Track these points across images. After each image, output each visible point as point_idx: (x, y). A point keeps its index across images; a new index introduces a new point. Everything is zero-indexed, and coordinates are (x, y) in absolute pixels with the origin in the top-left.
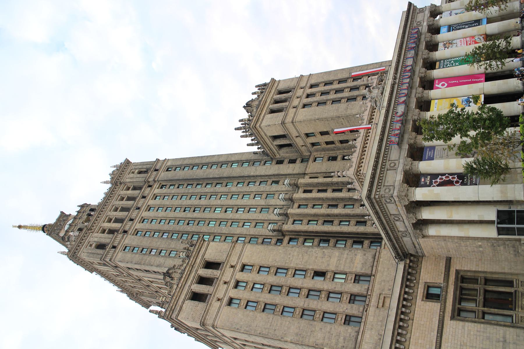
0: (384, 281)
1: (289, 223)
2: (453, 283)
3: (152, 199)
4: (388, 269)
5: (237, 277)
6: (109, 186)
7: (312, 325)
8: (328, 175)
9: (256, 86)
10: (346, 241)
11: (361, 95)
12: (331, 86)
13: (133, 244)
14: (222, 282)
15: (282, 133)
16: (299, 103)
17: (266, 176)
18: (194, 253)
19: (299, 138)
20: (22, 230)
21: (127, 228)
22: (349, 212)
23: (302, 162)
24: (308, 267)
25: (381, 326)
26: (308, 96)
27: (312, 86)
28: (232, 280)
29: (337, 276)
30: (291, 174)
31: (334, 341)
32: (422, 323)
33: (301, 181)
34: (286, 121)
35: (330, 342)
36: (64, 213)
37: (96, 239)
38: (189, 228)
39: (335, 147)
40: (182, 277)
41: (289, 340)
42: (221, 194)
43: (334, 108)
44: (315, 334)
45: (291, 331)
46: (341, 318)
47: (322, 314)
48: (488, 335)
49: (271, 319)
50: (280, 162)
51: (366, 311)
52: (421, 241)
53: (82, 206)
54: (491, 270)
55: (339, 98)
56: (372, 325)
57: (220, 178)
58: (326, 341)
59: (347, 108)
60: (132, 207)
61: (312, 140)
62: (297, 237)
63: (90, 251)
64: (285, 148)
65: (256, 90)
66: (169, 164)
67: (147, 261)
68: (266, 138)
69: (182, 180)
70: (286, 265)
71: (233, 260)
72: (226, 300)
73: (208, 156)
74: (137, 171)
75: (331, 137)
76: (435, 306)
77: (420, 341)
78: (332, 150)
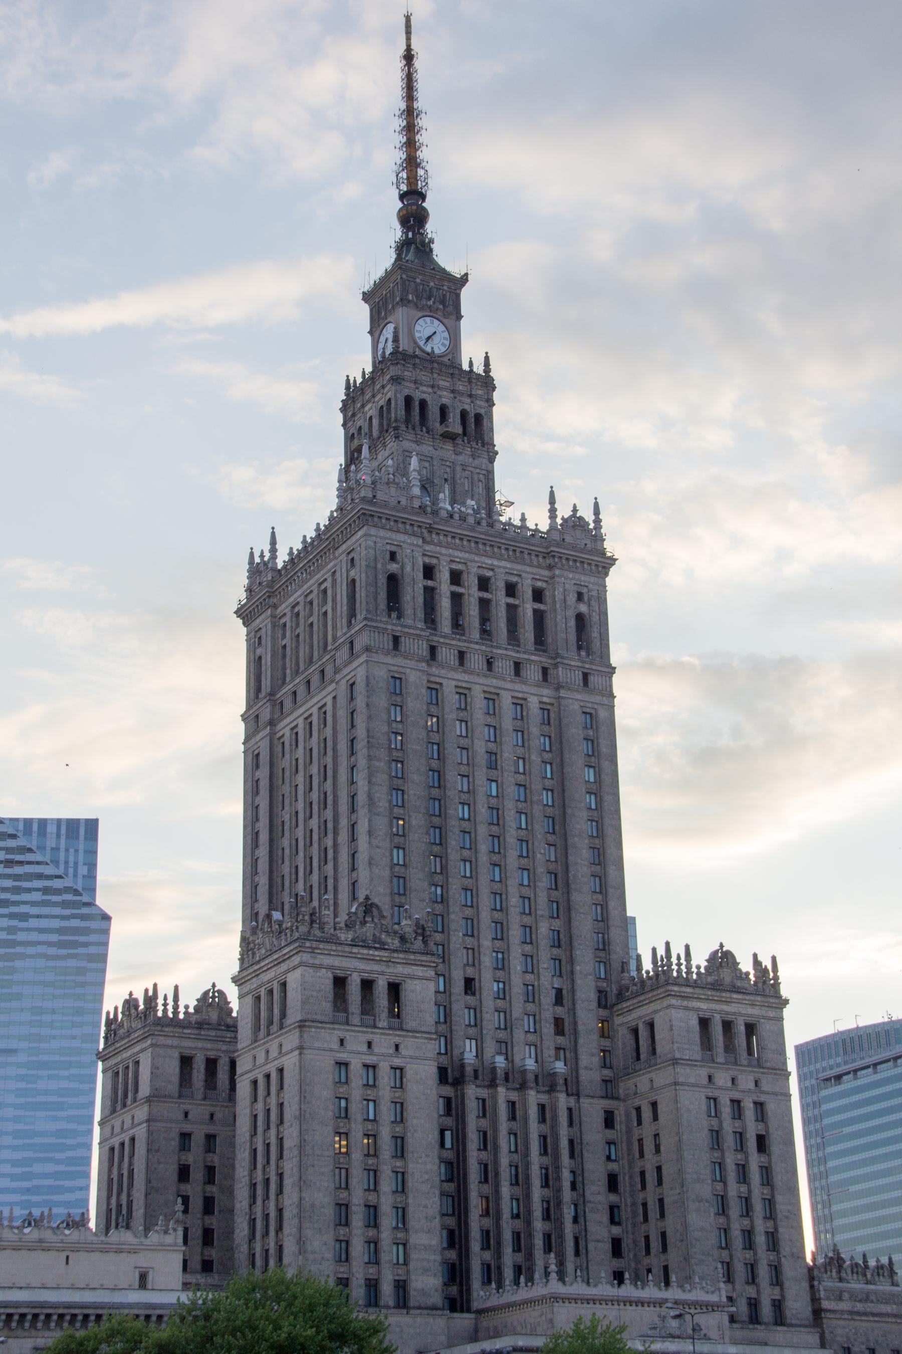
0: (402, 1331)
1: (479, 1090)
3: (512, 697)
6: (544, 526)
8: (577, 1148)
10: (453, 1214)
11: (728, 1225)
14: (370, 1037)
15: (659, 1050)
16: (720, 1088)
17: (574, 1004)
18: (412, 957)
19: (648, 1086)
20: (399, 64)
22: (505, 1217)
23: (605, 1081)
24: (411, 1195)
26: (736, 1103)
27: (760, 1106)
28: (375, 1058)
29: (401, 1248)
30: (577, 1064)
34: (679, 1069)
37: (408, 569)
38: (453, 843)
40: (370, 948)
41: (303, 1195)
44: (318, 1236)
57: (567, 885)
61: (647, 1114)
62: (454, 1112)
63: (379, 566)
64: (633, 1042)
66: (602, 714)
67: (377, 763)
69: (563, 773)
70: (410, 1155)
71: (410, 1046)
72: (343, 1056)
74: (583, 608)
75: (650, 1156)
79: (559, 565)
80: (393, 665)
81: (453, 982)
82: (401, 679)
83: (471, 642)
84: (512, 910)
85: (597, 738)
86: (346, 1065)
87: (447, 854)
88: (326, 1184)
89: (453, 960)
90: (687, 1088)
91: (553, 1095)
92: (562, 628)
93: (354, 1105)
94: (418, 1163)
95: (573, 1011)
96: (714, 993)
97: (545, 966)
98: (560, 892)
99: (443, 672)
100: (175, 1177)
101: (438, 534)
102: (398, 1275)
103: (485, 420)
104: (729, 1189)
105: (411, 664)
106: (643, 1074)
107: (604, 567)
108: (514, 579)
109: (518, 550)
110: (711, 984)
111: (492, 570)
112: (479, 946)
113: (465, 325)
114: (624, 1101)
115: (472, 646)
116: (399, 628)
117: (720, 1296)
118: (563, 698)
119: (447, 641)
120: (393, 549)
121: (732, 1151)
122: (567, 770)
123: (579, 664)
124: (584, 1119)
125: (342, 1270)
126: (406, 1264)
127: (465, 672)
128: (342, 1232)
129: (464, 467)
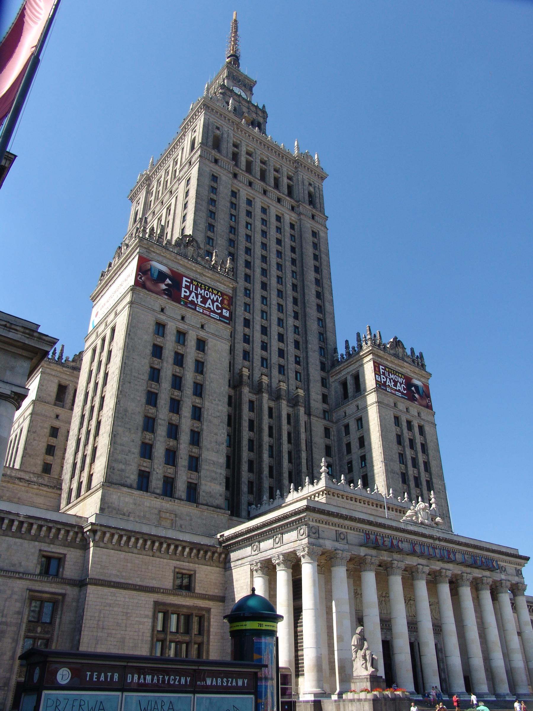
0: (191, 520)
1: (250, 394)
2: (195, 605)
3: (276, 211)
4: (205, 525)
5: (190, 332)
7: (137, 429)
9: (421, 354)
13: (221, 187)
16: (400, 411)
21: (240, 177)
22: (265, 473)
24: (205, 424)
25: (139, 516)
26: (409, 423)
27: (421, 428)
28: (186, 327)
30: (309, 397)
31: (119, 457)
32: (150, 568)
33: (302, 410)
35: (118, 452)
36: (255, 85)
37: (225, 136)
39: (343, 454)
43: (394, 456)
45: (129, 404)
46: (146, 464)
47: (150, 442)
48: (140, 645)
49: (142, 377)
50: (324, 383)
51: (155, 497)
52: (247, 568)
53: (264, 111)
54: (211, 650)
55: (406, 462)
56: (139, 505)
57: (304, 303)
58: (119, 448)
59: (394, 473)
60: (267, 184)
61: (353, 426)
63: (210, 128)
64: (342, 390)
65: (417, 353)
66: (322, 234)
68: (357, 366)
69: (302, 251)
72: (162, 318)
73: (331, 286)
74: (312, 189)
75: (357, 450)
76: (168, 583)
77: (129, 565)
78: (340, 451)
81: (236, 332)
84: (273, 306)
87: (237, 267)
88: (138, 398)
89: (237, 320)
91: (296, 408)
93: (167, 352)
94: (212, 403)
95: (307, 369)
97: (291, 341)
98: (300, 307)
99: (241, 185)
100: (44, 451)
102: (190, 478)
105: (225, 172)
106: (351, 403)
112: (253, 319)
114: (336, 423)
120: (219, 126)
122: (304, 250)
124: (313, 428)
125: (145, 464)
128: (148, 437)
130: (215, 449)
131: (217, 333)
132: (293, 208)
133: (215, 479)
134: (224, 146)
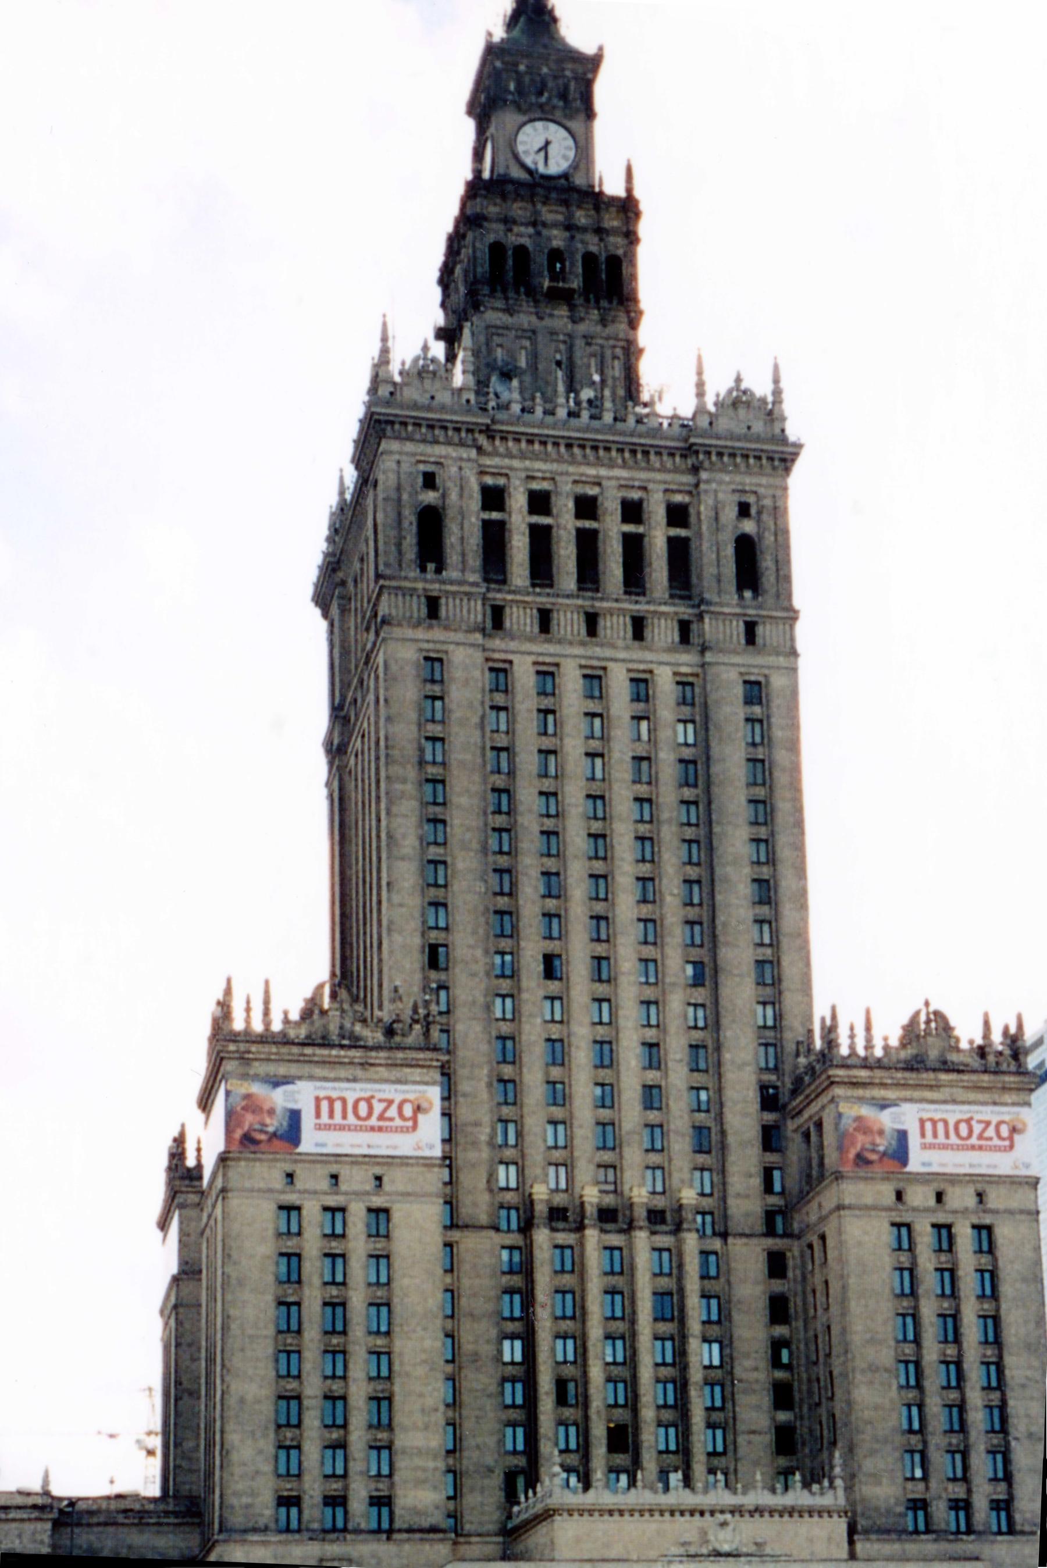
3: (629, 671)
12: (973, 1299)
16: (915, 1209)
27: (984, 1231)
30: (725, 1191)
42: (659, 957)
49: (265, 1332)
74: (748, 527)
79: (706, 464)
80: (428, 641)
82: (440, 660)
83: (558, 596)
85: (768, 717)
86: (298, 1209)
90: (857, 1212)
92: (714, 559)
96: (907, 1075)
99: (513, 645)
101: (504, 439)
102: (377, 1490)
103: (624, 265)
104: (925, 1352)
105: (460, 637)
107: (783, 460)
108: (635, 495)
109: (639, 449)
110: (905, 1062)
111: (599, 484)
113: (601, 127)
115: (560, 600)
116: (437, 586)
117: (836, 1498)
118: (709, 664)
119: (518, 597)
121: (933, 1298)
123: (738, 610)
126: (390, 1476)
127: (549, 641)
129: (588, 340)
130: (420, 1424)
131: (409, 1189)
132: (685, 629)
133: (425, 1481)
134: (452, 537)
